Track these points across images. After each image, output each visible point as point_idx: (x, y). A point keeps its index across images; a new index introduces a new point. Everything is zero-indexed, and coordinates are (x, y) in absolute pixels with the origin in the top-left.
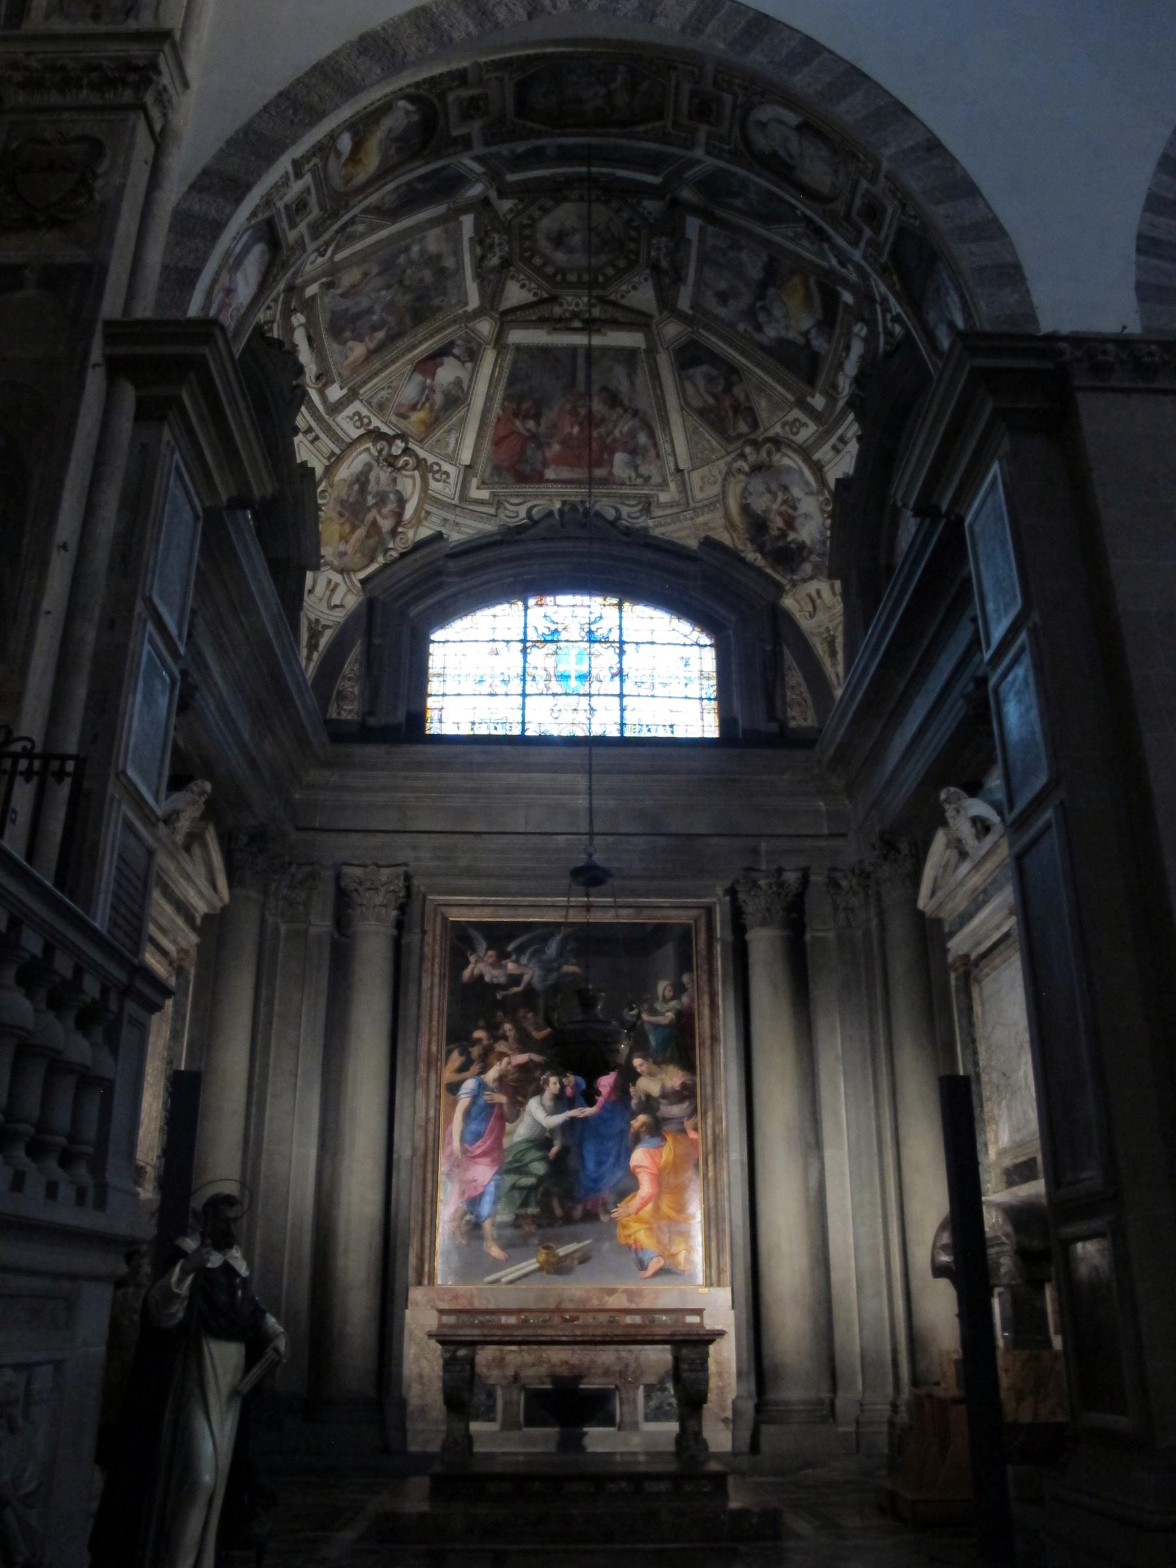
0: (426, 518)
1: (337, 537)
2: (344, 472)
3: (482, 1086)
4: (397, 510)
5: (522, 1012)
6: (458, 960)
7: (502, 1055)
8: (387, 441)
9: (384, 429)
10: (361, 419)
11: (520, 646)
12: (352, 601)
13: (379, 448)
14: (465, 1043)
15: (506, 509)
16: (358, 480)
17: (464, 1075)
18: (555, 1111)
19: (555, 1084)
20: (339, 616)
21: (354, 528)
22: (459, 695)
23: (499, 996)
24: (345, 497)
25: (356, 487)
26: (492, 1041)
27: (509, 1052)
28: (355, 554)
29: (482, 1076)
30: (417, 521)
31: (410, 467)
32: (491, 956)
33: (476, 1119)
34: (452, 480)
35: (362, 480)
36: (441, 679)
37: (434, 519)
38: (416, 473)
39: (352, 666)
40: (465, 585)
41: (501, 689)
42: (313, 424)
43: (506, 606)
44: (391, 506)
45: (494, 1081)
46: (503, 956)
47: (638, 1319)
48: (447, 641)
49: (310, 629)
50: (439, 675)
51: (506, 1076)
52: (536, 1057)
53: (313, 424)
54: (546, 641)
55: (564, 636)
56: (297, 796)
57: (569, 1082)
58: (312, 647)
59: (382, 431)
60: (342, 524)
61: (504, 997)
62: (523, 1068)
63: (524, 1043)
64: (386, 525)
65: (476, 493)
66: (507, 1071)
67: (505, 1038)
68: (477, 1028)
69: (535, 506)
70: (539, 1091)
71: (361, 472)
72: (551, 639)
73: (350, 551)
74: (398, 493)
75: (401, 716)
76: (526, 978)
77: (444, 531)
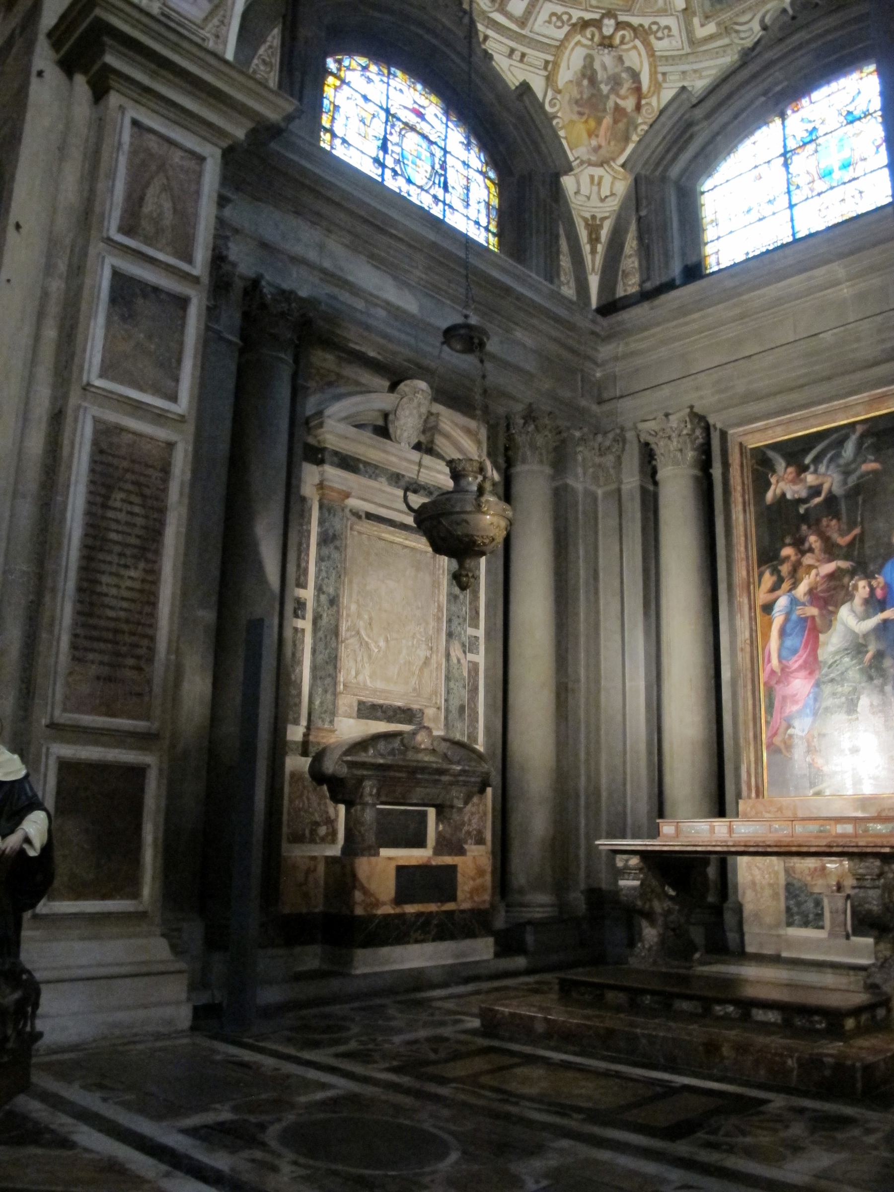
0: (665, 81)
1: (585, 135)
2: (566, 75)
3: (794, 602)
4: (634, 86)
5: (824, 522)
6: (761, 484)
7: (810, 567)
8: (594, 26)
9: (588, 16)
10: (559, 18)
11: (782, 159)
12: (622, 187)
13: (589, 36)
14: (775, 563)
15: (737, 32)
16: (584, 75)
17: (778, 593)
18: (867, 616)
19: (864, 587)
20: (613, 204)
21: (599, 122)
22: (731, 232)
23: (802, 511)
24: (579, 97)
25: (585, 82)
26: (800, 556)
27: (817, 564)
28: (609, 143)
29: (793, 592)
30: (657, 86)
31: (627, 39)
32: (791, 473)
33: (790, 635)
34: (675, 31)
35: (588, 74)
36: (714, 224)
37: (672, 78)
39: (631, 244)
40: (715, 126)
41: (767, 210)
42: (513, 44)
43: (764, 129)
44: (627, 84)
45: (805, 594)
46: (803, 469)
47: (849, 828)
48: (715, 187)
49: (587, 225)
50: (712, 221)
51: (816, 588)
52: (844, 564)
53: (513, 44)
54: (805, 144)
55: (821, 132)
56: (598, 375)
57: (879, 583)
58: (594, 240)
60: (586, 122)
61: (807, 510)
62: (831, 576)
63: (831, 551)
64: (629, 104)
65: (701, 32)
66: (817, 583)
67: (811, 550)
68: (784, 545)
69: (763, 17)
70: (849, 597)
71: (584, 67)
72: (811, 139)
73: (603, 144)
75: (676, 269)
76: (826, 487)
77: (686, 84)
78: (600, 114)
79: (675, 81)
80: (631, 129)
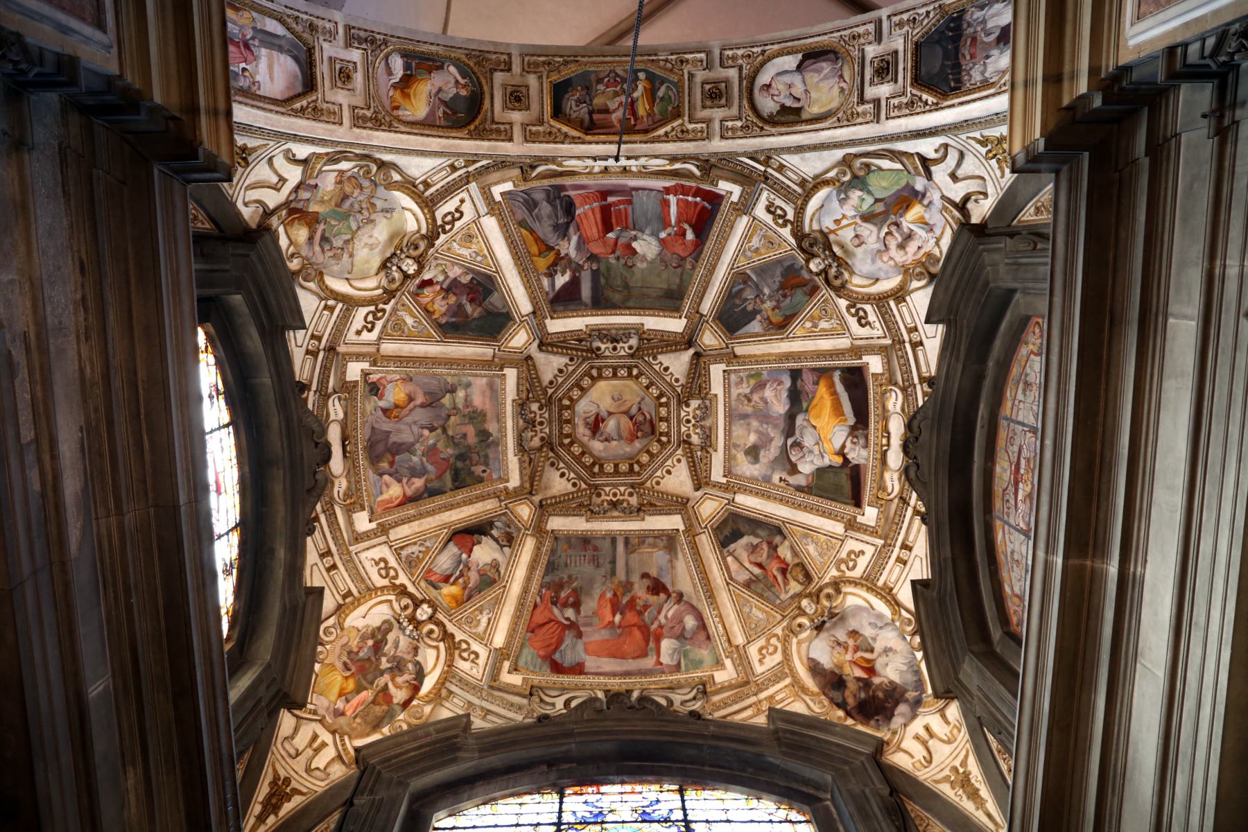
35: (378, 637)
38: (441, 645)
64: (399, 695)
74: (418, 664)
78: (364, 683)
79: (456, 705)
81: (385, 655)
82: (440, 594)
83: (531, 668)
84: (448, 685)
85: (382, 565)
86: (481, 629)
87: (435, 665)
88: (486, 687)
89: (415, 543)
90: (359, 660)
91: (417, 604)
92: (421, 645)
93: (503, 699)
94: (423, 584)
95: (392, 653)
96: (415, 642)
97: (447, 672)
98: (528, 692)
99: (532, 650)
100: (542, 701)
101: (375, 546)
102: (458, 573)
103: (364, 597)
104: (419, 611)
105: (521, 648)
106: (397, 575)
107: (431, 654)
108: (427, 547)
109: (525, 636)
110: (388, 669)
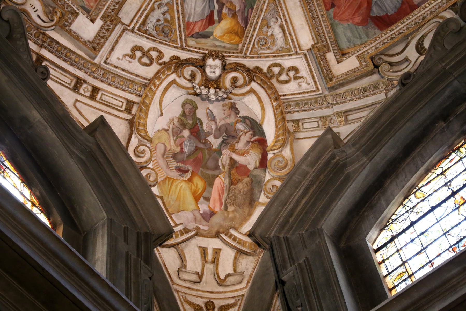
38: (254, 85)
59: (182, 58)
74: (245, 118)
79: (311, 129)
80: (256, 191)
81: (209, 134)
82: (215, 39)
83: (358, 42)
84: (288, 117)
85: (138, 54)
86: (280, 41)
87: (263, 108)
88: (326, 93)
89: (153, 9)
90: (189, 155)
91: (202, 66)
92: (235, 99)
93: (351, 92)
94: (191, 42)
95: (214, 127)
96: (227, 101)
97: (279, 106)
98: (372, 67)
99: (345, 24)
100: (391, 64)
101: (117, 42)
102: (216, 6)
103: (147, 96)
104: (208, 70)
105: (334, 30)
106: (160, 53)
107: (251, 101)
108: (167, 4)
109: (328, 15)
110: (221, 144)
